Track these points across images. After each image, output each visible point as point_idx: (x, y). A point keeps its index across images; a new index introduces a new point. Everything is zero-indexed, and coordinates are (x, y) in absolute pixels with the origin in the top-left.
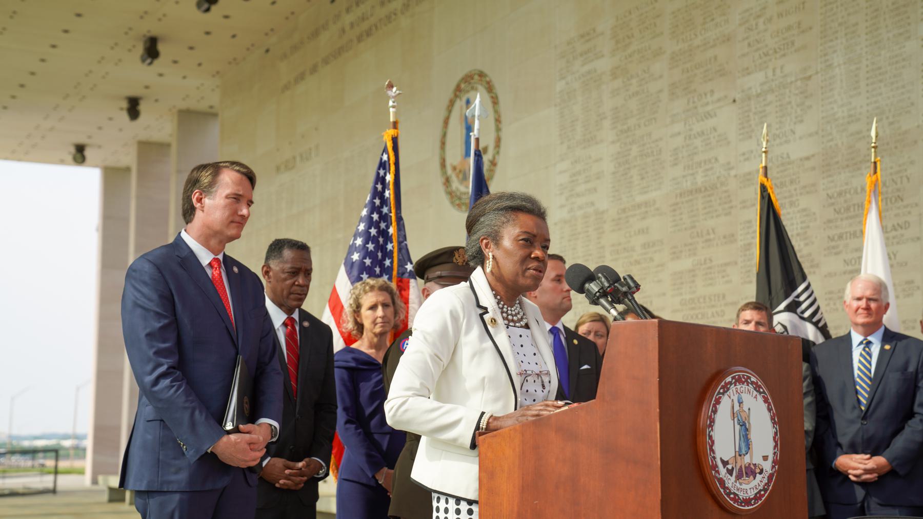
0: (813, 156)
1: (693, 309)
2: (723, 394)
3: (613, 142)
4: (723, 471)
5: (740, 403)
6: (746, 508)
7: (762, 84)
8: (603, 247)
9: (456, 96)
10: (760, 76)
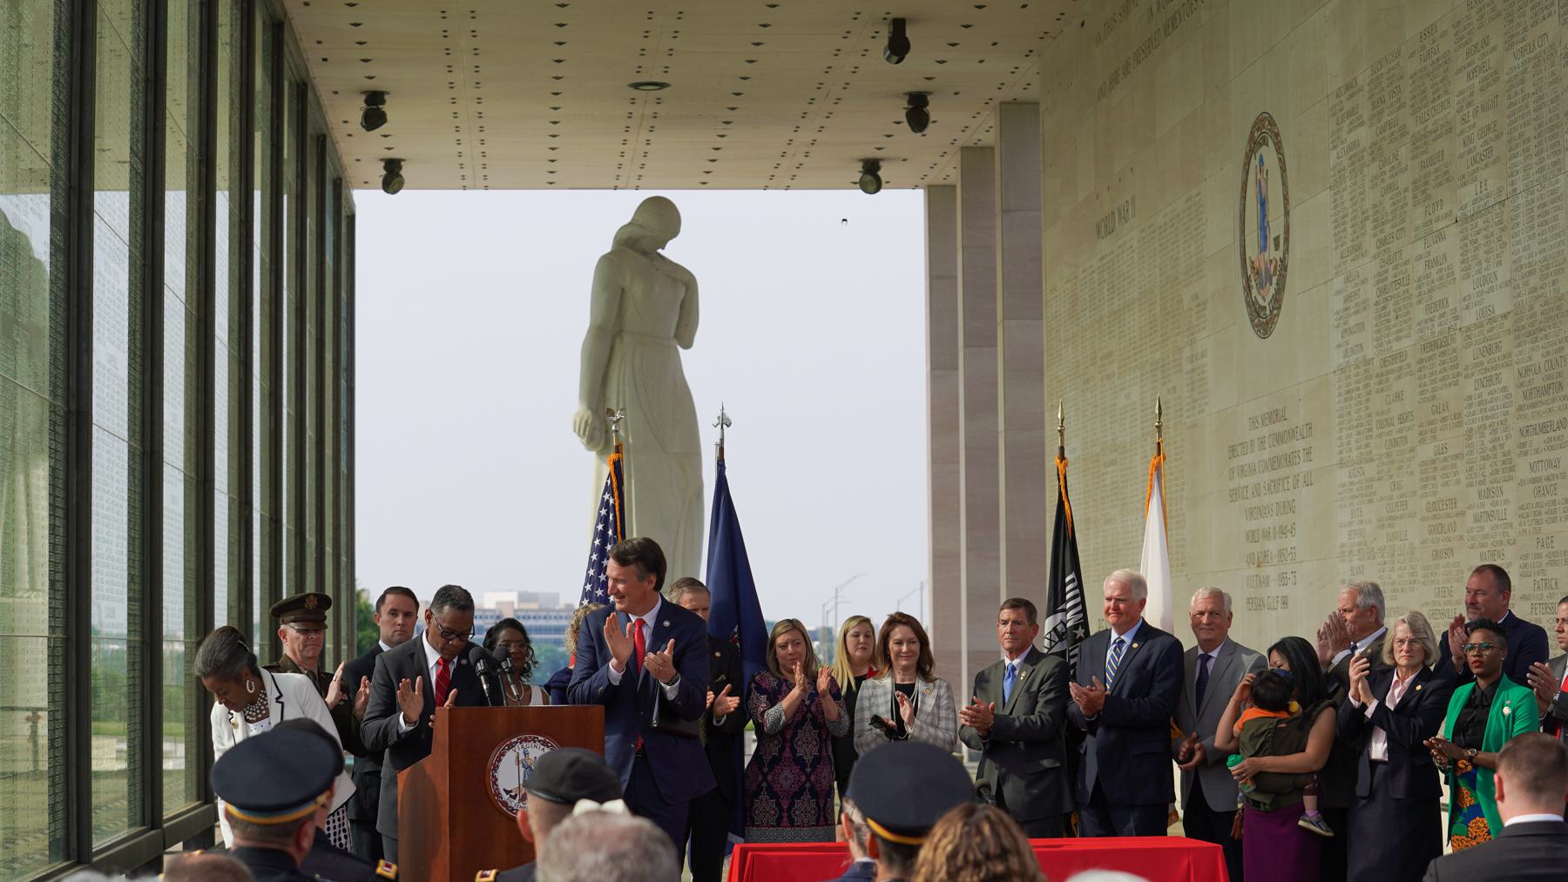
0: (1509, 313)
1: (1435, 517)
2: (508, 749)
3: (1375, 257)
4: (505, 797)
5: (526, 754)
7: (1475, 201)
8: (1369, 415)
9: (1251, 152)
10: (1471, 188)
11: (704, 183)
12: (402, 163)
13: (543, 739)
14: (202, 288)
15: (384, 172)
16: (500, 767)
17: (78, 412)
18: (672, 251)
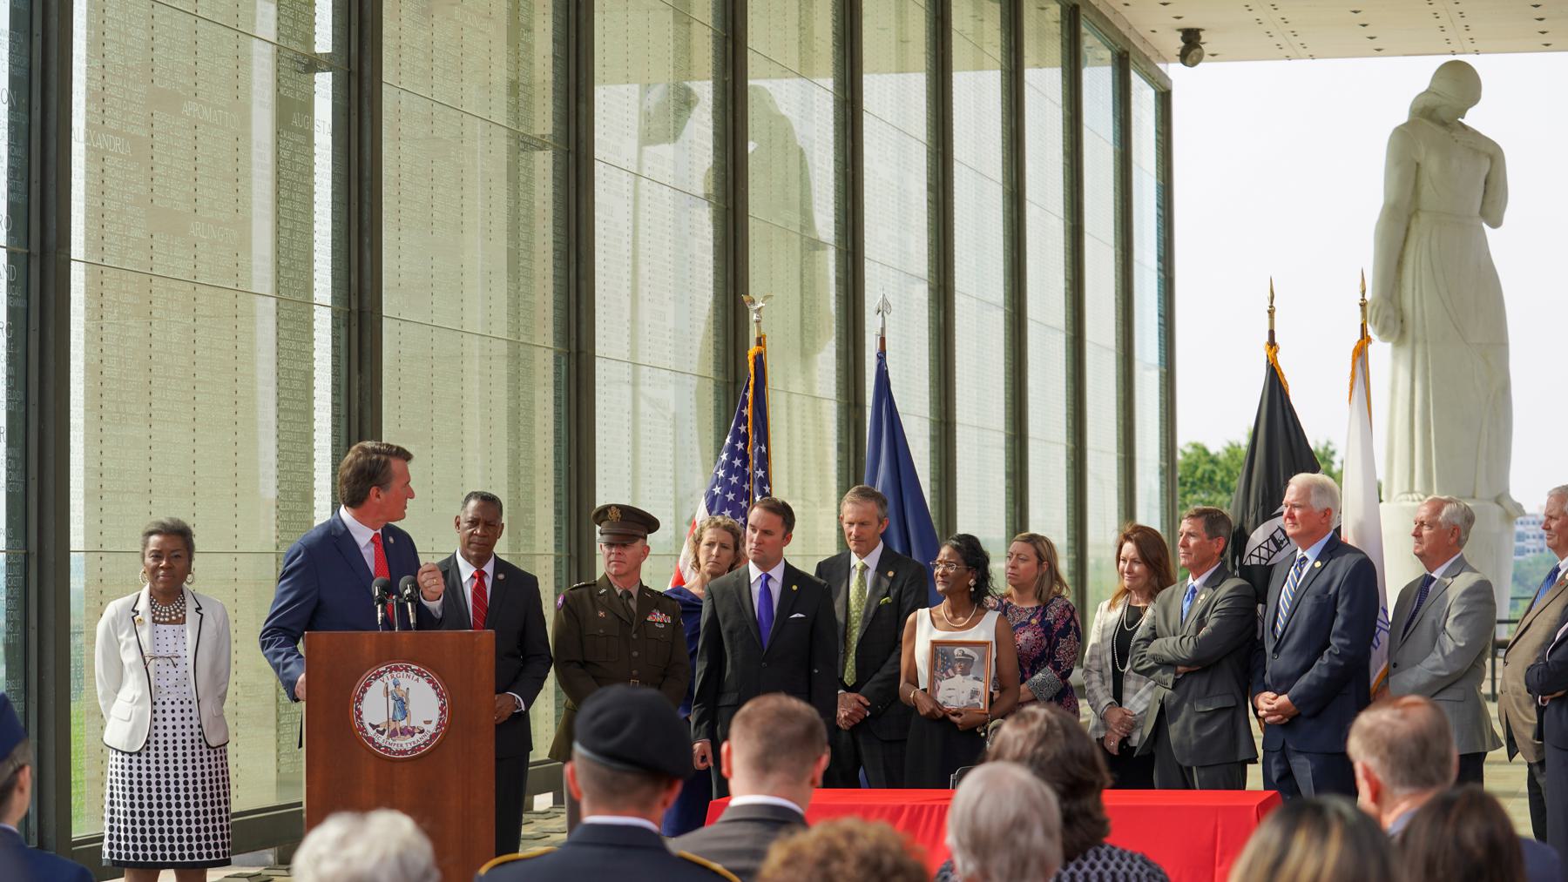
2: (375, 679)
4: (372, 732)
6: (401, 756)
11: (1547, 45)
12: (1201, 33)
13: (417, 668)
14: (730, 174)
15: (1182, 44)
16: (365, 700)
17: (361, 312)
18: (1472, 118)
